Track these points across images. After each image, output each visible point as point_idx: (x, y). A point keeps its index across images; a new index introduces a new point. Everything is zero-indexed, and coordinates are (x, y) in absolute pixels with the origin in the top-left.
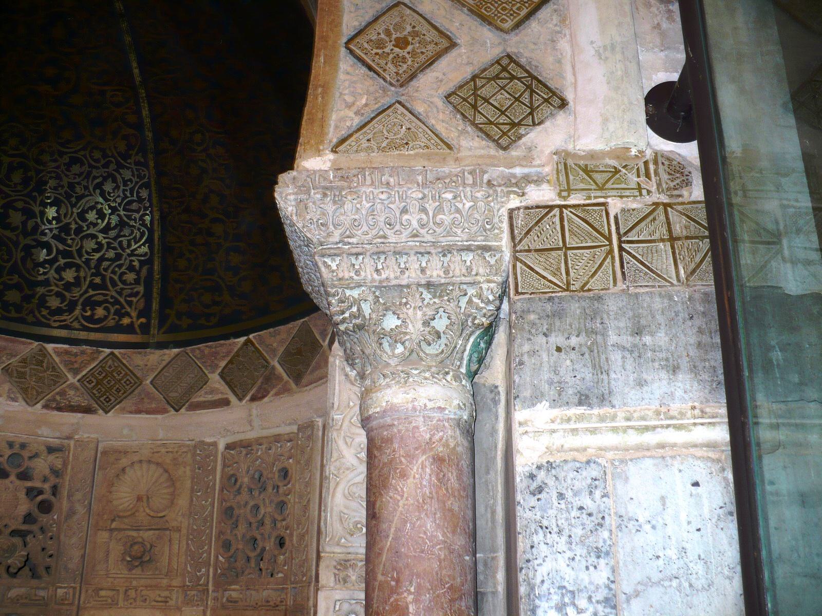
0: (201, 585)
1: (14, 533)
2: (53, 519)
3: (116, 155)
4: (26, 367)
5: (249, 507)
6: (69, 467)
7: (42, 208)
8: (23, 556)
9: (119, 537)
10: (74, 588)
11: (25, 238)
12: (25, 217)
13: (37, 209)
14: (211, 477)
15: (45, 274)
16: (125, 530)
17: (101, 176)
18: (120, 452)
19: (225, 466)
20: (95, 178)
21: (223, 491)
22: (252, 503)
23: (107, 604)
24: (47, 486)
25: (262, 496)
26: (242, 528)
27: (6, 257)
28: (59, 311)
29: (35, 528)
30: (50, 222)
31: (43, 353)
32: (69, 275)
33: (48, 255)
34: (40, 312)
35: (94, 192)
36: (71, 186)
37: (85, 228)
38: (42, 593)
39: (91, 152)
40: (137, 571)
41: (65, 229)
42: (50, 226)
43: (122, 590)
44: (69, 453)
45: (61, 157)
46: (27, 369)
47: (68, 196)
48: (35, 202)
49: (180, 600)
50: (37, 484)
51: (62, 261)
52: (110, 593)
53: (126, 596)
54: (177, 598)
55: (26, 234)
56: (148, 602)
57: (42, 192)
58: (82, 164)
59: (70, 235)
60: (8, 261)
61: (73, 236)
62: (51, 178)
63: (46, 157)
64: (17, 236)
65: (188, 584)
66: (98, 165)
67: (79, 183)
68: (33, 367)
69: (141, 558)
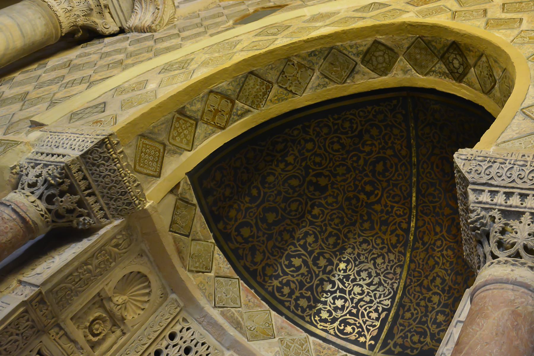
3: (389, 244)
4: (293, 344)
7: (338, 262)
11: (323, 274)
12: (327, 263)
13: (335, 262)
15: (326, 298)
17: (377, 254)
20: (373, 254)
27: (308, 280)
28: (325, 321)
30: (340, 271)
31: (306, 340)
32: (339, 303)
33: (332, 288)
34: (314, 317)
35: (370, 261)
36: (359, 255)
37: (358, 280)
39: (376, 239)
41: (347, 277)
42: (339, 273)
45: (359, 237)
46: (293, 345)
47: (355, 260)
48: (336, 257)
51: (338, 294)
55: (324, 272)
57: (342, 253)
58: (369, 244)
59: (348, 281)
60: (309, 283)
61: (350, 282)
62: (349, 247)
63: (350, 235)
64: (319, 272)
66: (378, 247)
67: (363, 255)
68: (297, 345)
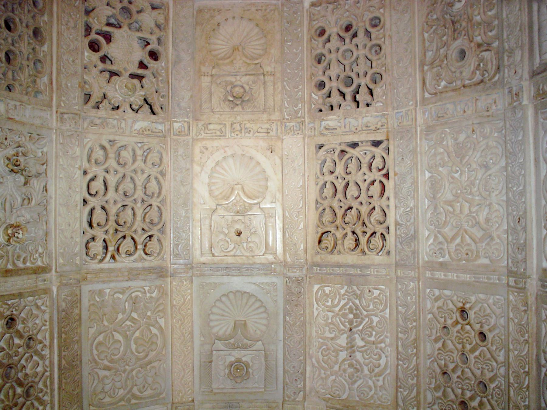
0: (299, 118)
1: (133, 76)
2: (162, 66)
8: (142, 96)
9: (219, 82)
14: (299, 30)
18: (214, 10)
19: (311, 20)
21: (311, 41)
23: (216, 136)
26: (334, 71)
38: (160, 127)
40: (238, 109)
44: (168, 10)
49: (279, 131)
50: (147, 36)
52: (218, 127)
53: (233, 130)
54: (277, 130)
56: (252, 133)
65: (286, 117)
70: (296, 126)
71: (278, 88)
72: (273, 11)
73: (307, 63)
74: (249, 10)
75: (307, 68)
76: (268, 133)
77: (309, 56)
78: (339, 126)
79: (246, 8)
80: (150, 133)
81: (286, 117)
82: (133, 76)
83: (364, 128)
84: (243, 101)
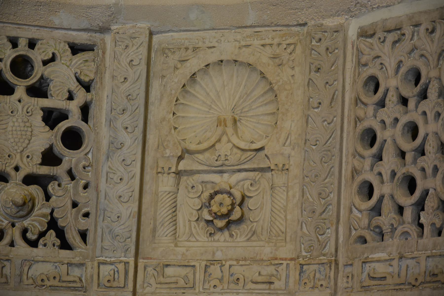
0: (324, 255)
1: (29, 180)
5: (400, 125)
6: (107, 76)
8: (44, 216)
10: (126, 263)
16: (199, 172)
22: (404, 120)
24: (74, 107)
25: (420, 110)
29: (59, 171)
43: (200, 266)
52: (183, 271)
54: (288, 277)
69: (230, 212)
70: (320, 272)
71: (294, 196)
72: (292, 47)
73: (347, 149)
74: (247, 46)
75: (347, 156)
76: (271, 283)
77: (351, 134)
78: (390, 274)
79: (243, 43)
80: (56, 283)
81: (304, 254)
82: (29, 180)
83: (428, 279)
84: (229, 223)
